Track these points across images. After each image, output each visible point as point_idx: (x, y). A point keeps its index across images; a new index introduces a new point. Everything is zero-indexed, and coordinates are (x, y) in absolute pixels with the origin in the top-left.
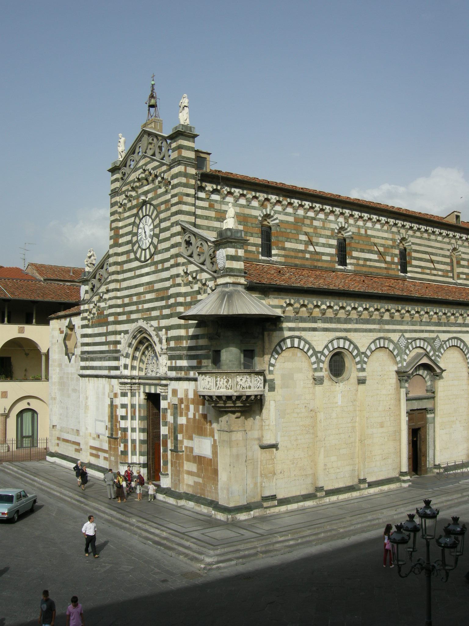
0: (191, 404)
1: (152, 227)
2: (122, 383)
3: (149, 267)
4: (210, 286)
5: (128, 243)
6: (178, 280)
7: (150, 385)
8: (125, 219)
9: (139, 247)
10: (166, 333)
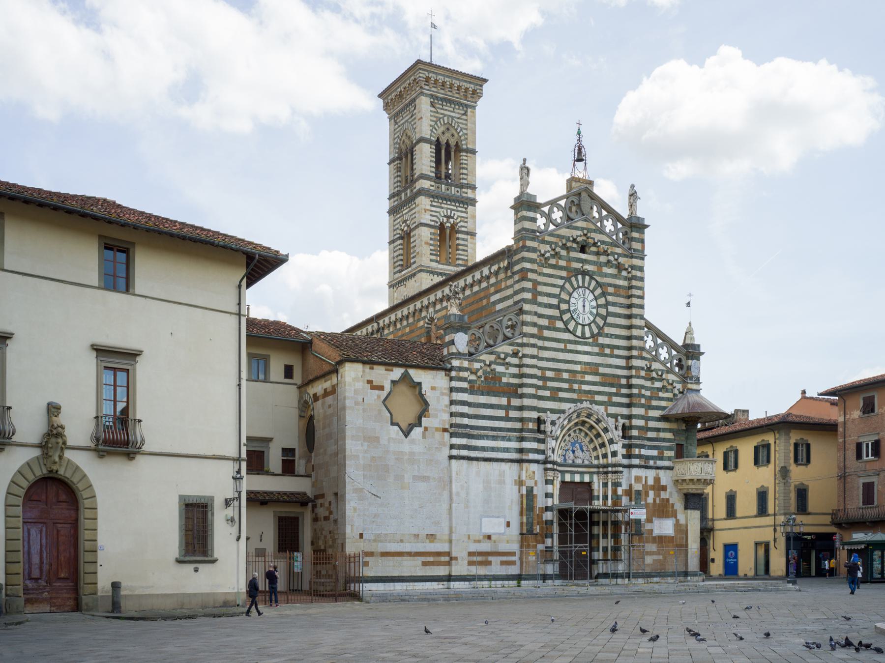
0: (650, 490)
1: (594, 303)
3: (590, 347)
4: (677, 388)
5: (550, 306)
6: (643, 373)
7: (572, 473)
8: (544, 275)
9: (572, 317)
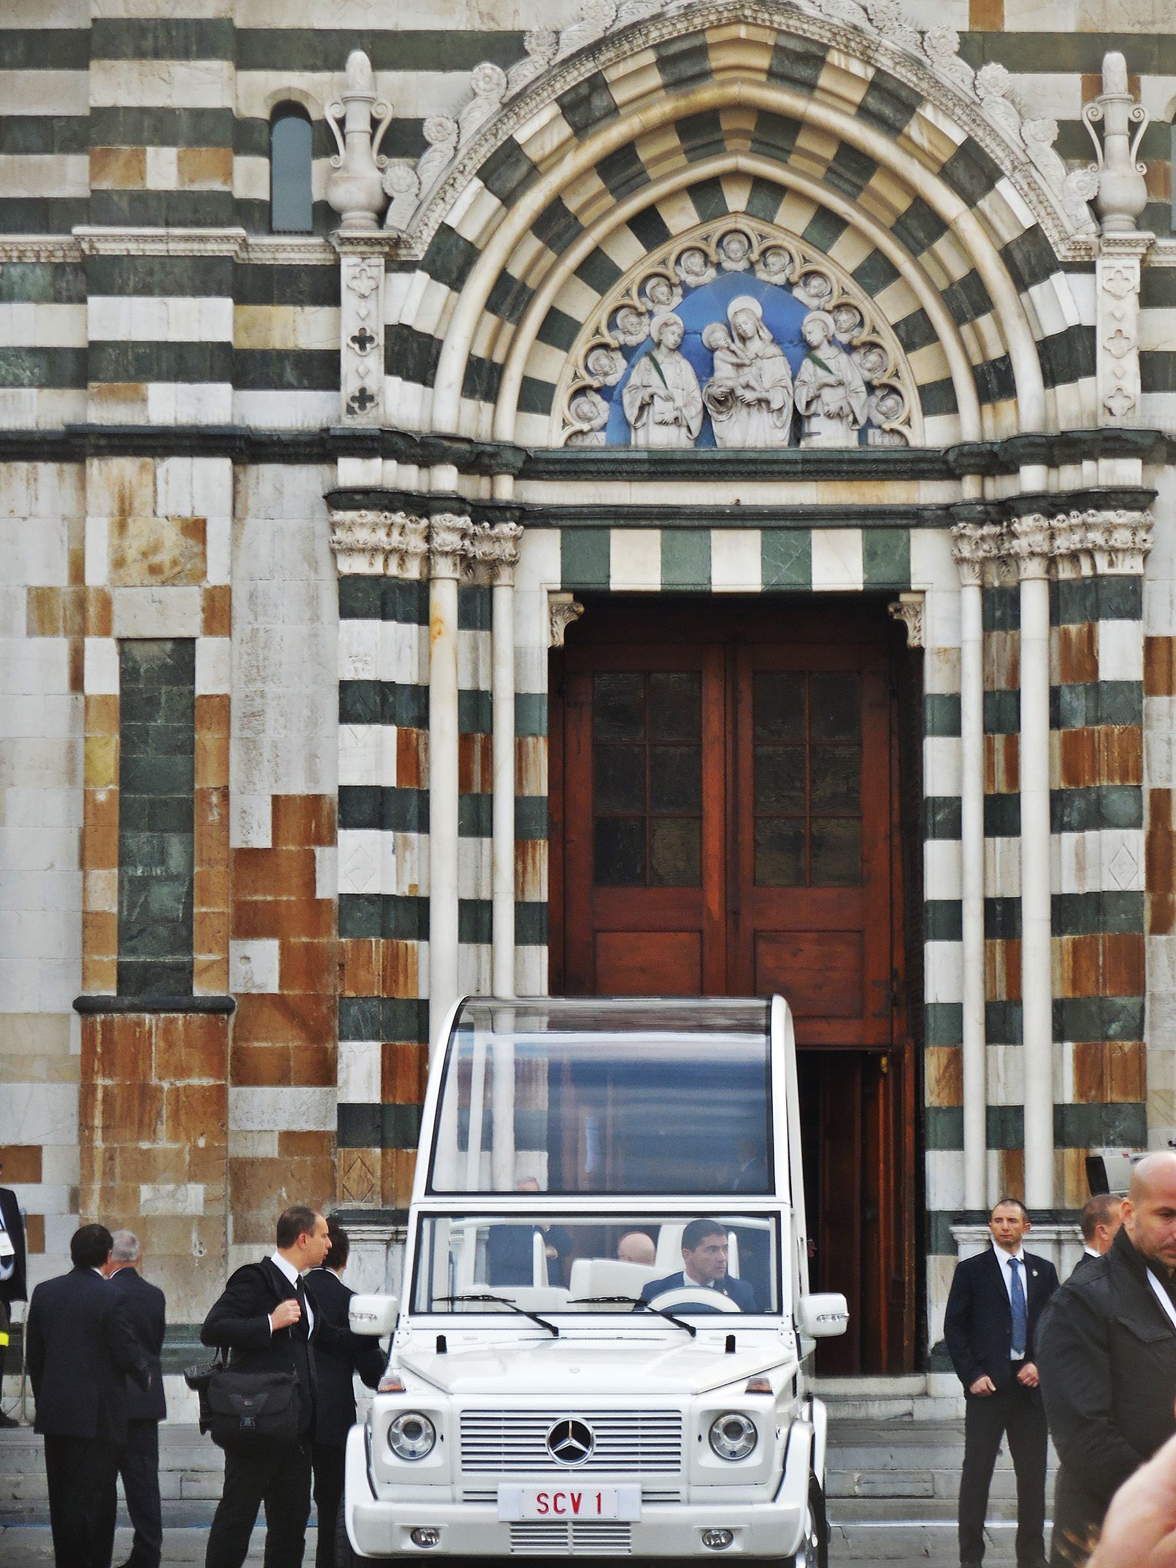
2: (339, 499)
10: (1134, 87)
